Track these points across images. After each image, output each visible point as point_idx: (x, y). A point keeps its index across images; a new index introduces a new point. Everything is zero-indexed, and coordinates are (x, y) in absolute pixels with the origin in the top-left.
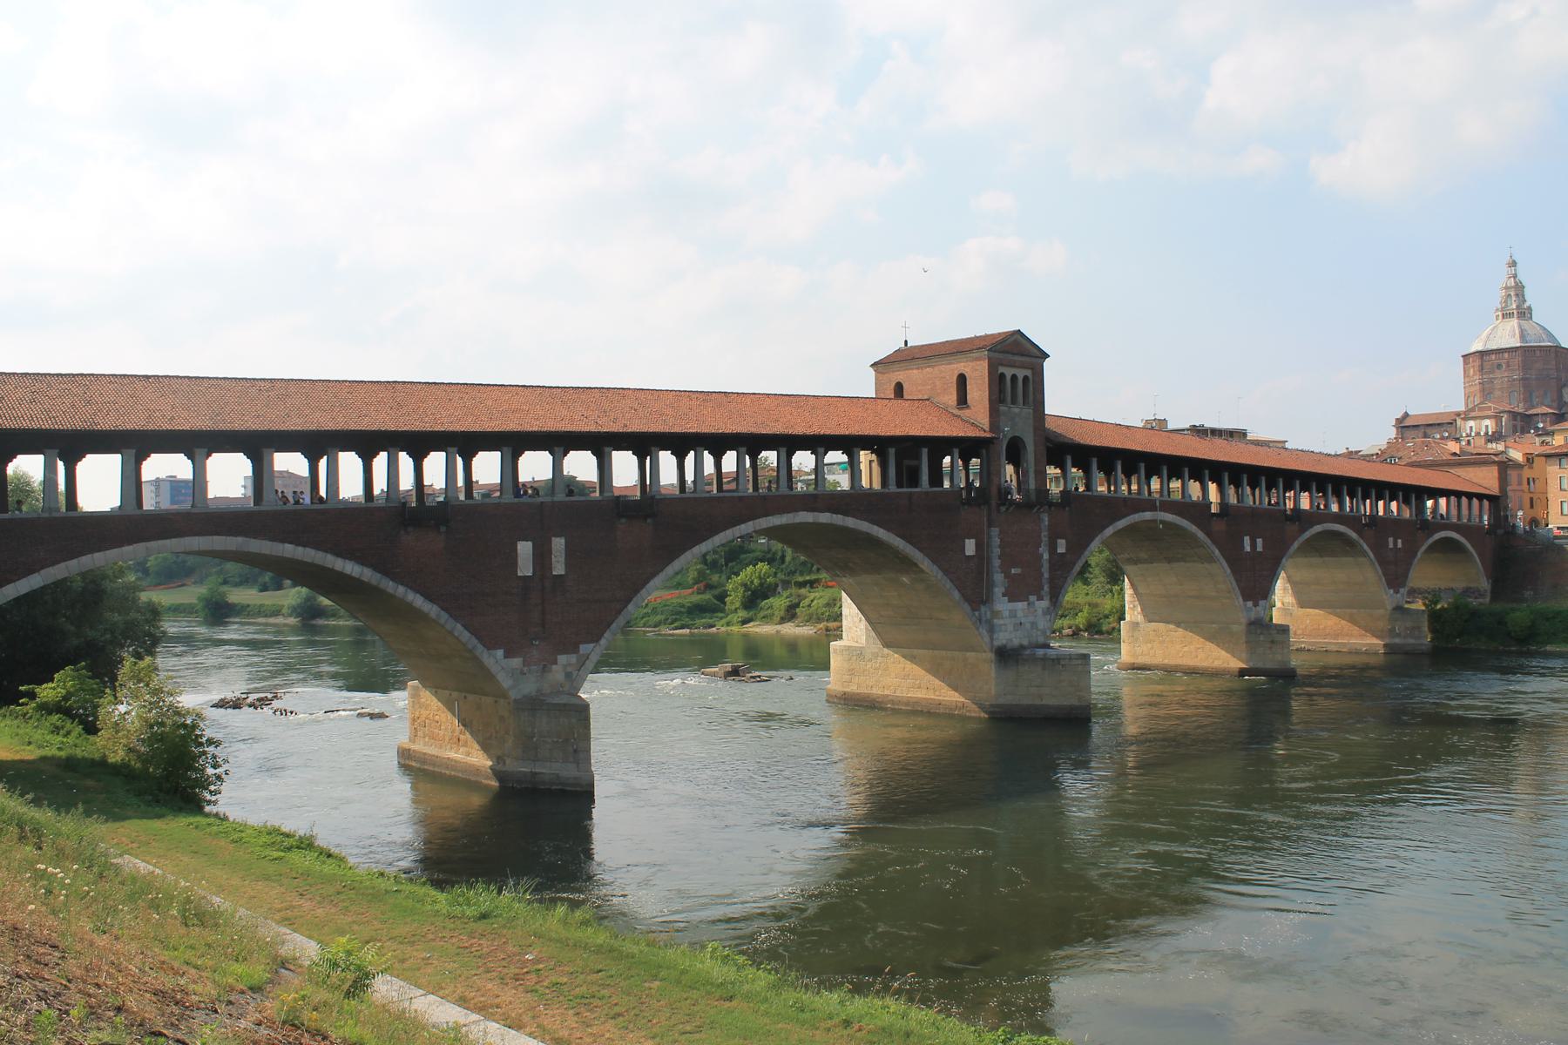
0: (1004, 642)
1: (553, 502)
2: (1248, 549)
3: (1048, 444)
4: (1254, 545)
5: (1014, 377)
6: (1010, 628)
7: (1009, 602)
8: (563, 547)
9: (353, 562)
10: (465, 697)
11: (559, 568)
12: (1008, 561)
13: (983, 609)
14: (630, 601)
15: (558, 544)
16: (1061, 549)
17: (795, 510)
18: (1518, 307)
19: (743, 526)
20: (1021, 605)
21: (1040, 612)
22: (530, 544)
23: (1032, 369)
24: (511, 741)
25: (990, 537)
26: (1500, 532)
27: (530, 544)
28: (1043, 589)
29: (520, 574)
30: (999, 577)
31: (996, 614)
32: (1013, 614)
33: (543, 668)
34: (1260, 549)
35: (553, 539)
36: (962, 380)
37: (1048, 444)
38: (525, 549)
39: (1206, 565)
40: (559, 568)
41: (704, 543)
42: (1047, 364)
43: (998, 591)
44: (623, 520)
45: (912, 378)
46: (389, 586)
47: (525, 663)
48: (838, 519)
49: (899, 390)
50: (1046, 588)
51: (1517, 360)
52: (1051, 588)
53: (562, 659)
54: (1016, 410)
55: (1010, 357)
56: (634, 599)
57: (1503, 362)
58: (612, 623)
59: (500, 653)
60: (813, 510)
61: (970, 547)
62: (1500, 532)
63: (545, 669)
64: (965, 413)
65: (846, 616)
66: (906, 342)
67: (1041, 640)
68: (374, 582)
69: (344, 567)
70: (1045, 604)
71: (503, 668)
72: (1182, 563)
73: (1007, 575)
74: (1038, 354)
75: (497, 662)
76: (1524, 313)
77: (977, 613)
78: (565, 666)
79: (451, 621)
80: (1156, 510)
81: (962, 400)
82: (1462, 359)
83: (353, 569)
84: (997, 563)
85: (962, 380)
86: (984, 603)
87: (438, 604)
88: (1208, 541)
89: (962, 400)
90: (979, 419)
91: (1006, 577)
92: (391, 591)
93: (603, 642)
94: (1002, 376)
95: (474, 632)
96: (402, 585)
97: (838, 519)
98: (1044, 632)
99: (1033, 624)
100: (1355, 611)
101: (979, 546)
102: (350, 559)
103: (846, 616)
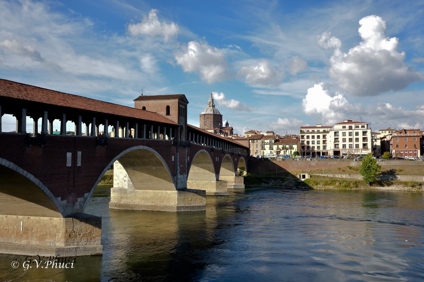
1: (78, 137)
2: (216, 160)
3: (188, 129)
5: (182, 108)
6: (180, 183)
7: (180, 175)
8: (81, 155)
9: (6, 160)
10: (28, 218)
11: (79, 164)
12: (180, 164)
13: (175, 177)
14: (99, 176)
15: (79, 153)
16: (188, 160)
18: (212, 105)
19: (128, 149)
20: (182, 176)
22: (71, 153)
23: (185, 106)
24: (60, 235)
25: (177, 155)
26: (249, 157)
27: (71, 153)
29: (67, 166)
30: (178, 167)
31: (177, 178)
32: (181, 179)
33: (73, 203)
34: (218, 160)
35: (78, 152)
36: (168, 108)
37: (188, 129)
38: (69, 155)
39: (208, 165)
40: (79, 164)
41: (118, 155)
42: (188, 105)
43: (178, 172)
44: (99, 146)
45: (150, 105)
46: (21, 171)
47: (68, 202)
49: (144, 108)
50: (186, 171)
51: (212, 117)
52: (187, 171)
53: (79, 200)
54: (182, 118)
56: (100, 176)
57: (209, 117)
58: (94, 184)
59: (60, 198)
60: (143, 145)
62: (249, 157)
64: (168, 117)
65: (116, 180)
66: (142, 94)
68: (15, 169)
69: (2, 162)
71: (60, 205)
72: (201, 164)
73: (180, 167)
74: (186, 102)
75: (58, 203)
76: (213, 106)
77: (174, 179)
78: (80, 202)
79: (43, 186)
81: (168, 113)
82: (199, 116)
83: (6, 163)
84: (178, 163)
85: (168, 108)
86: (175, 175)
87: (39, 179)
89: (168, 113)
90: (174, 120)
91: (180, 168)
92: (21, 173)
93: (91, 192)
94: (180, 107)
95: (51, 191)
96: (26, 170)
100: (226, 177)
102: (4, 158)
103: (116, 180)
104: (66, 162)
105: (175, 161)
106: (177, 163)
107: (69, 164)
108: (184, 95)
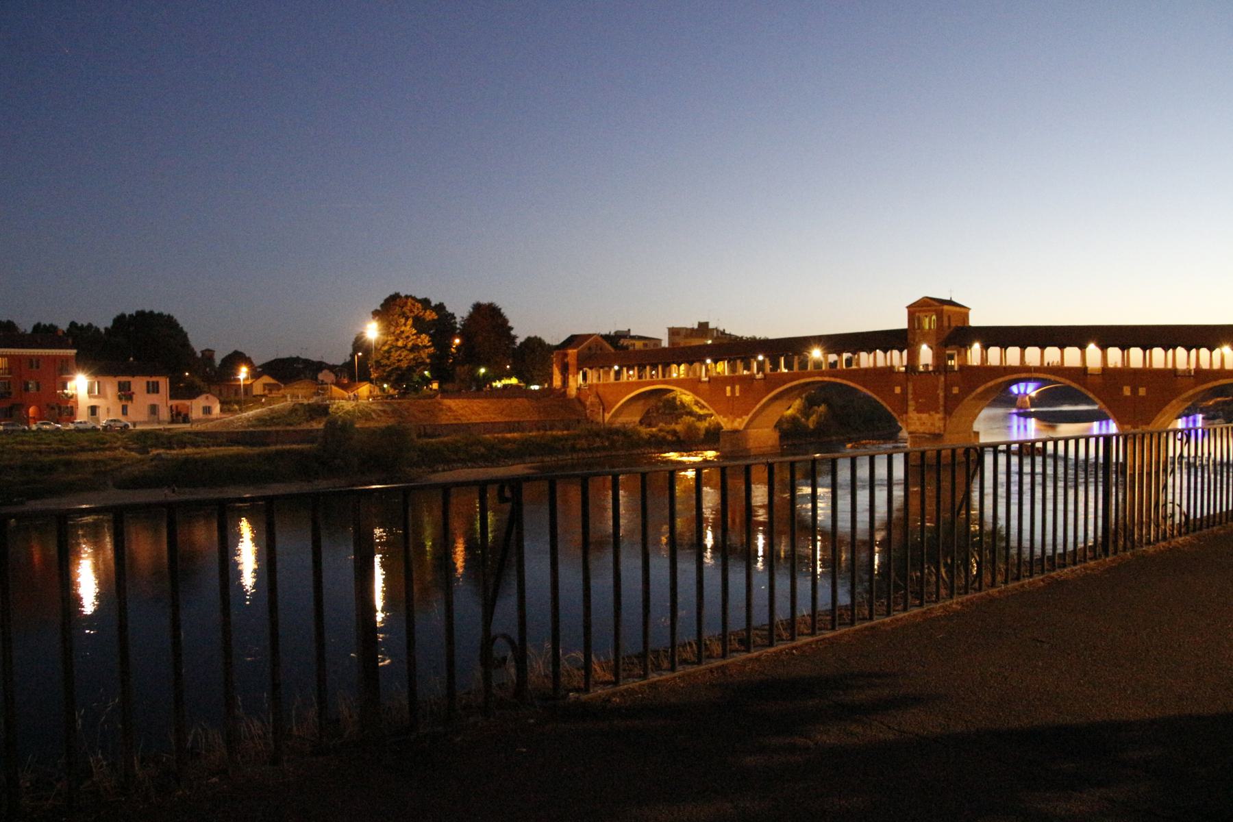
0: (914, 430)
4: (1134, 391)
7: (918, 412)
11: (737, 394)
12: (916, 396)
13: (904, 416)
15: (737, 387)
17: (814, 376)
20: (924, 416)
21: (937, 419)
28: (939, 408)
38: (728, 388)
40: (737, 394)
43: (911, 409)
48: (833, 379)
50: (941, 408)
55: (920, 309)
59: (721, 417)
60: (821, 376)
61: (898, 390)
63: (733, 422)
67: (937, 431)
70: (940, 415)
73: (917, 402)
80: (1031, 372)
88: (1083, 390)
97: (833, 379)
98: (939, 428)
99: (933, 425)
101: (901, 389)
104: (726, 394)
105: (904, 396)
106: (907, 397)
107: (728, 394)
108: (923, 298)
